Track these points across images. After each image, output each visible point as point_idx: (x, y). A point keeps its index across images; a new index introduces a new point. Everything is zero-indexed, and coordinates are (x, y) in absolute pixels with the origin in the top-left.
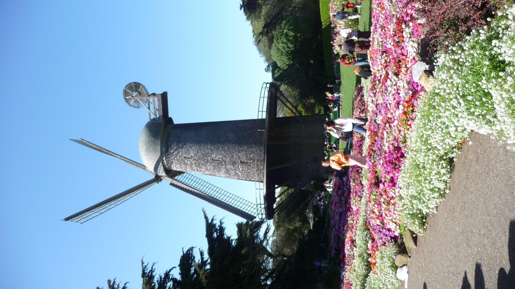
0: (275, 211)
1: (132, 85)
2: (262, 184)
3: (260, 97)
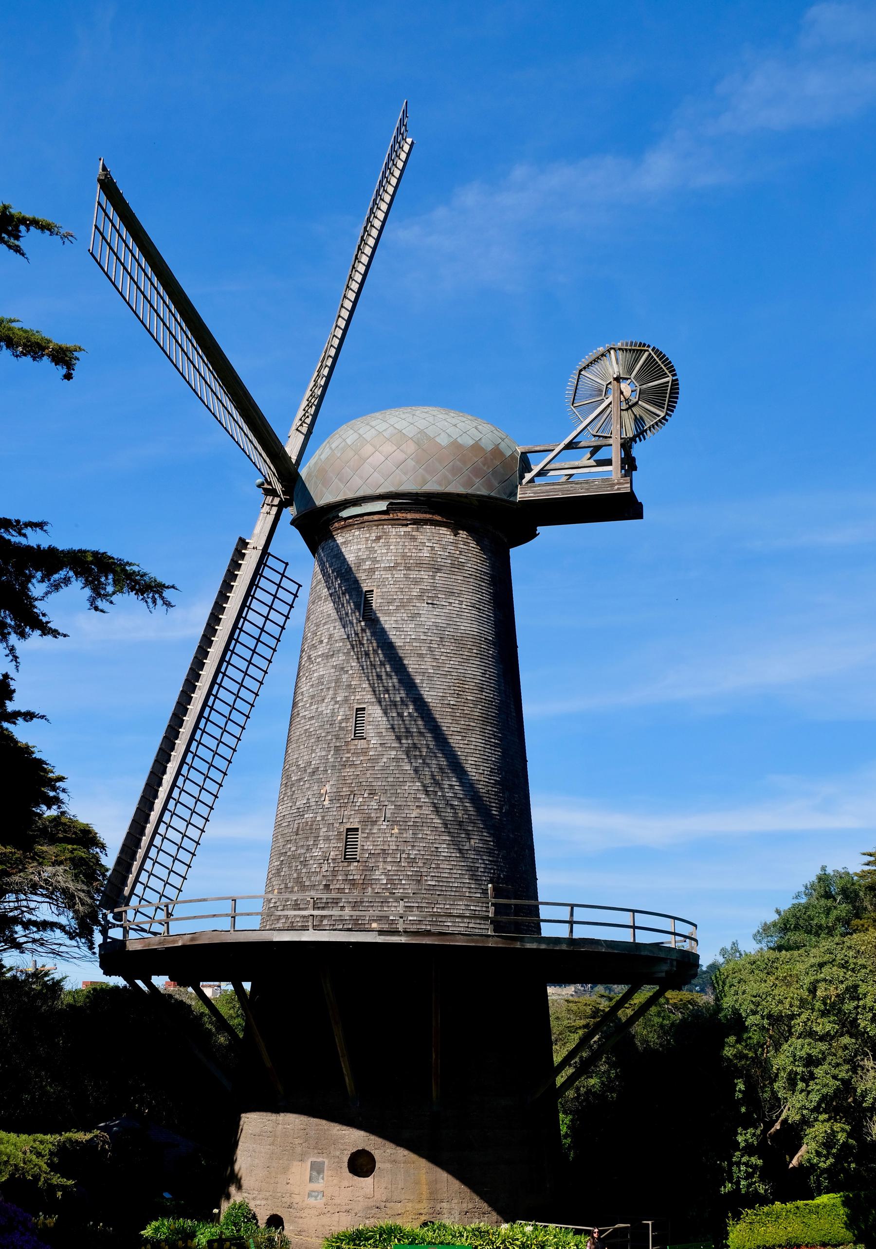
1: (665, 375)
2: (255, 922)
3: (634, 911)
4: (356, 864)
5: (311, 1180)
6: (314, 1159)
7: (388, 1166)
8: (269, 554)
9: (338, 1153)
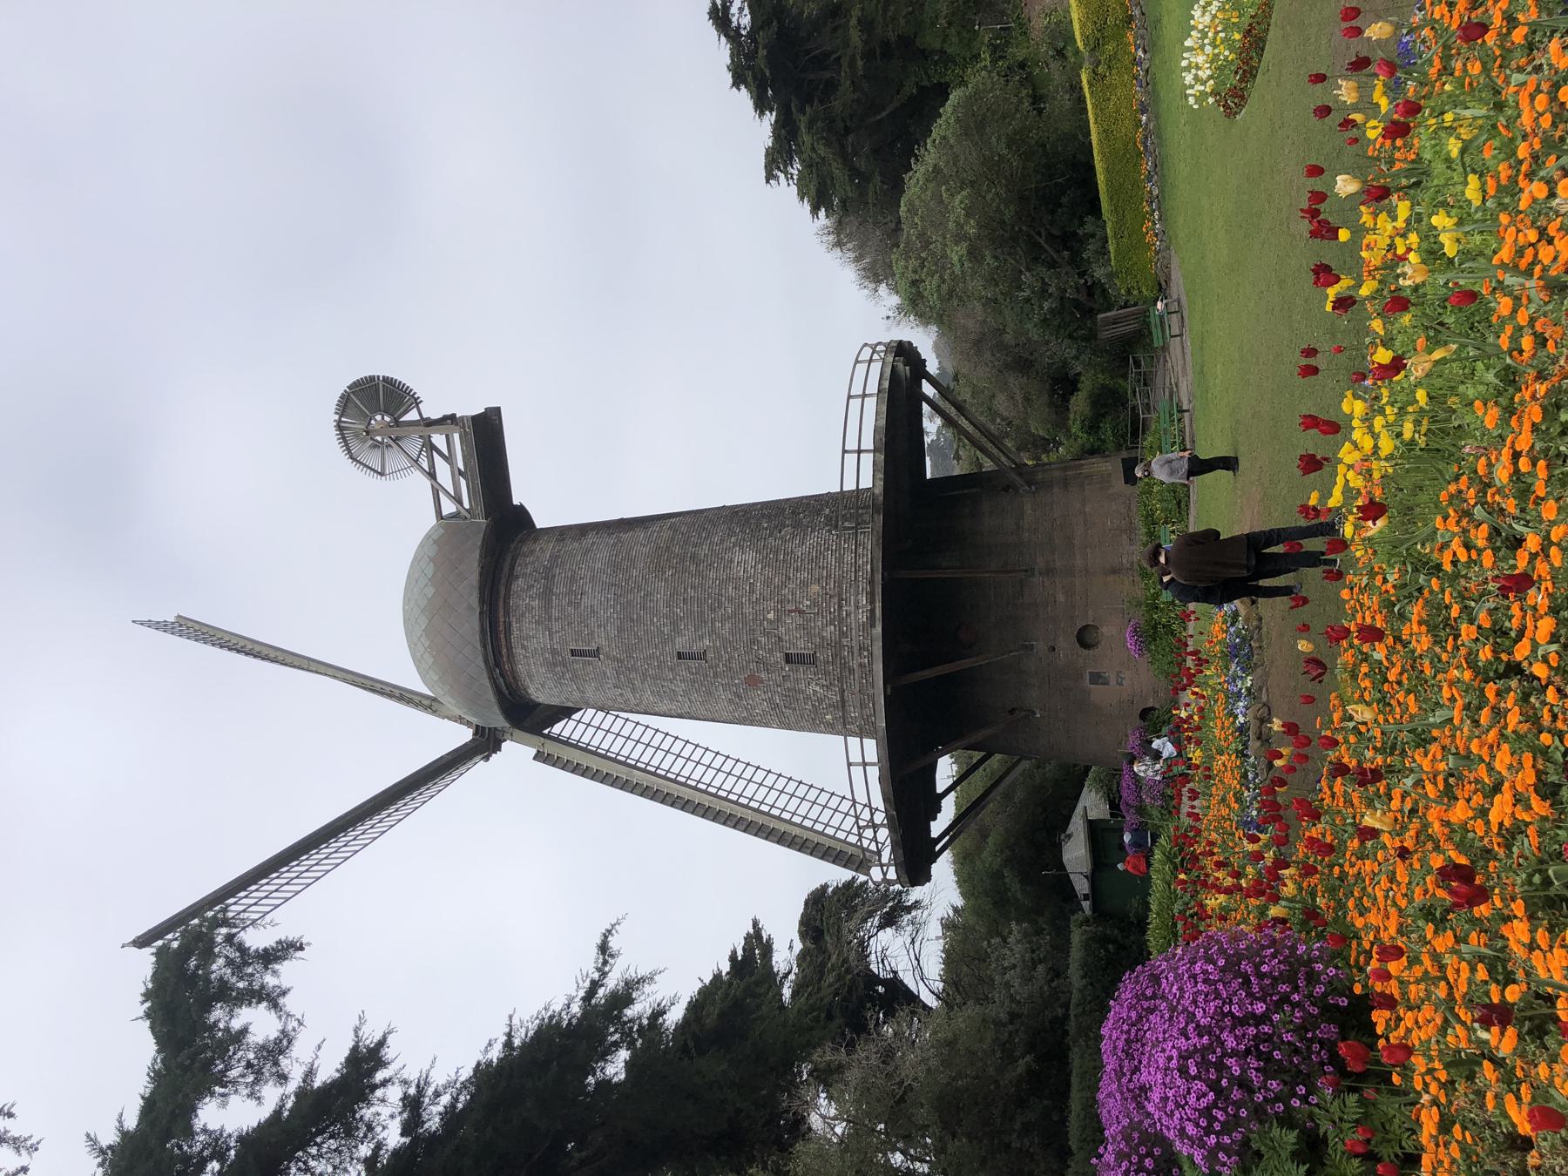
0: (937, 848)
4: (818, 655)
5: (1106, 683)
6: (1088, 681)
7: (1090, 613)
8: (485, 744)
9: (1081, 660)
